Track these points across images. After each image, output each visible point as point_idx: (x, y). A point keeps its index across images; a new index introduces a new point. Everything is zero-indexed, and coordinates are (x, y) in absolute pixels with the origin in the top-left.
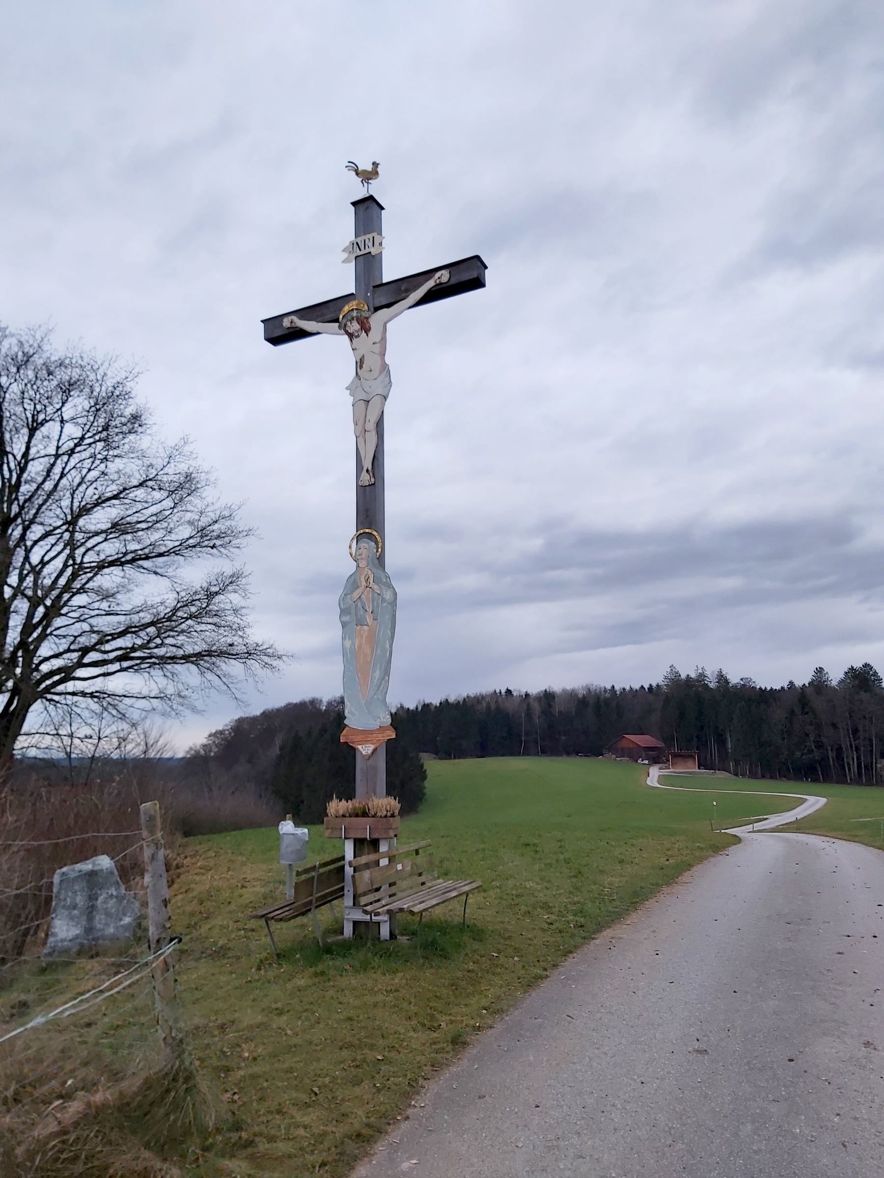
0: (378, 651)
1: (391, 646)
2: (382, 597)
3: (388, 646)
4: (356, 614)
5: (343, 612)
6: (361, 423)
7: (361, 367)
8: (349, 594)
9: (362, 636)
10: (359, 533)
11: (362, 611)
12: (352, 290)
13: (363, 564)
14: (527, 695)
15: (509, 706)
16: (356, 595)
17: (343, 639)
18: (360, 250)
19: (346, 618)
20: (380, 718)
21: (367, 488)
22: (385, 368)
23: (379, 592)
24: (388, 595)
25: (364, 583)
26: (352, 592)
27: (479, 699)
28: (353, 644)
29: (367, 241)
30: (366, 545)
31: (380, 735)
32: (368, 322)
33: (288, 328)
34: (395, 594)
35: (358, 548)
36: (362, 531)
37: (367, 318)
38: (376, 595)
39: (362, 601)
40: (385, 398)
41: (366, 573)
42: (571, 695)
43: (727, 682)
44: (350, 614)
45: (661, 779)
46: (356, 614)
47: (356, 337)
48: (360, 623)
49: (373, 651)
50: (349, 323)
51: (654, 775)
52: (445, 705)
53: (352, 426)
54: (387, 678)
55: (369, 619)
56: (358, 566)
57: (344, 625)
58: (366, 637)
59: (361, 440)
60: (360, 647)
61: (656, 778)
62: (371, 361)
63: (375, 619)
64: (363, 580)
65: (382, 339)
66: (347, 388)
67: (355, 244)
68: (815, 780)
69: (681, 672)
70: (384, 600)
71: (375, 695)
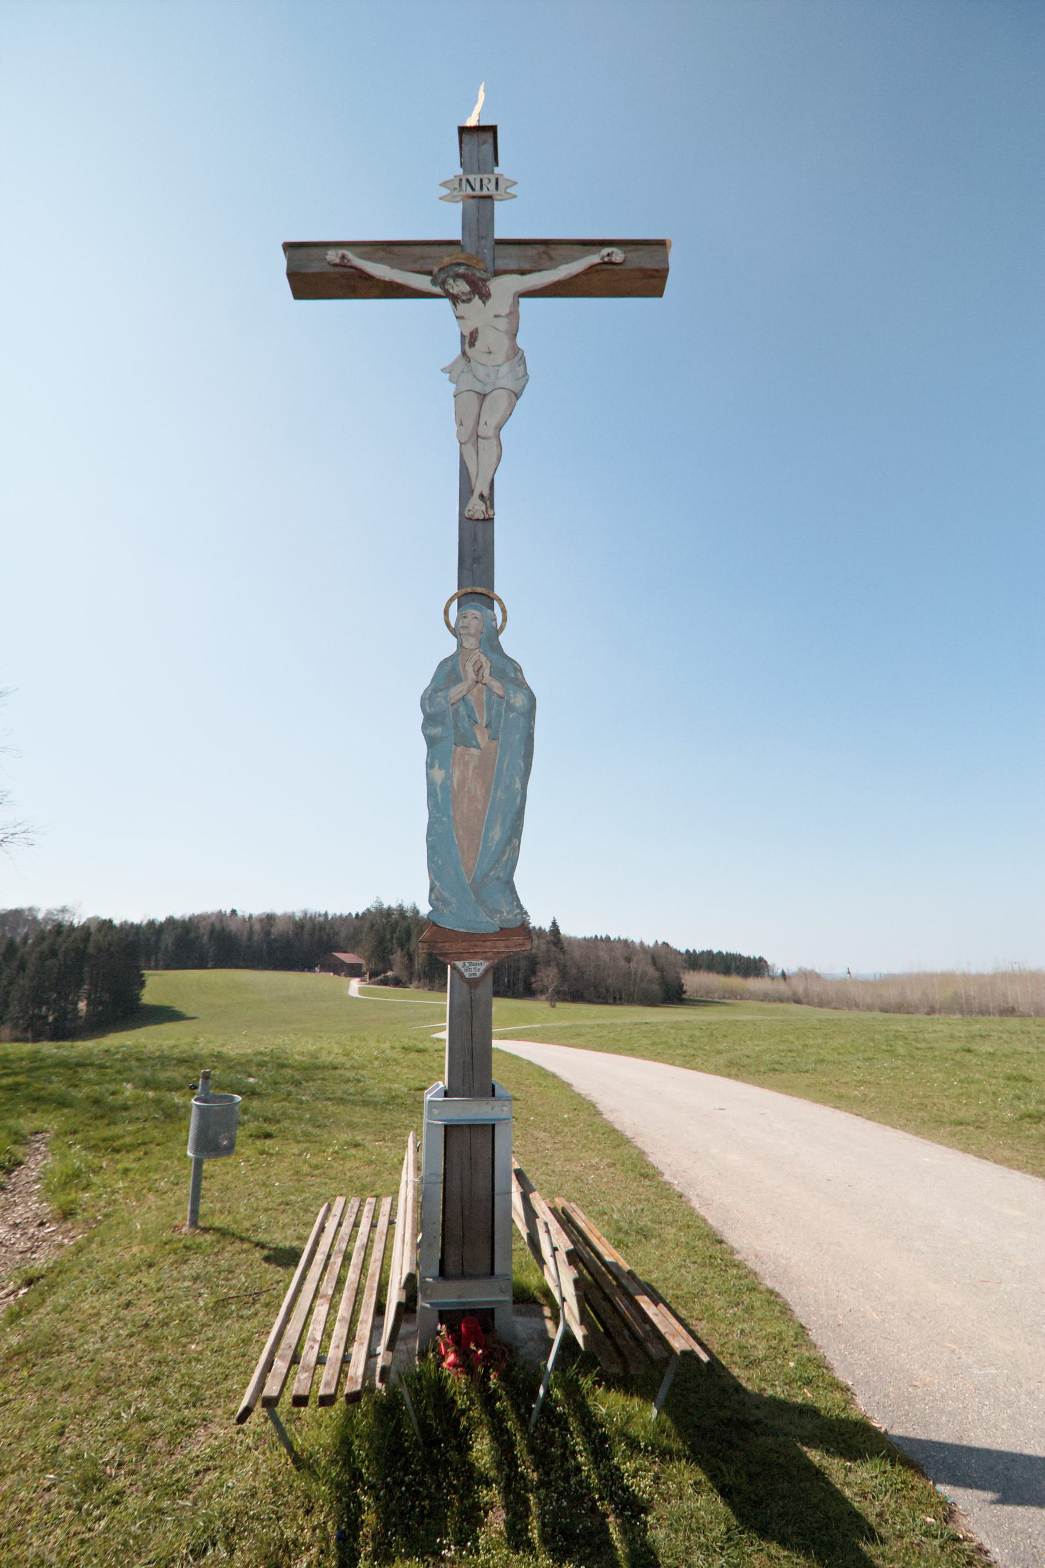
0: (499, 794)
1: (524, 788)
2: (508, 703)
3: (518, 786)
4: (456, 727)
5: (430, 720)
6: (470, 423)
7: (472, 344)
8: (441, 690)
9: (466, 765)
10: (463, 591)
11: (466, 724)
12: (456, 235)
13: (470, 643)
14: (250, 917)
15: (233, 927)
16: (456, 692)
17: (430, 766)
18: (481, 180)
19: (437, 731)
20: (502, 913)
21: (479, 523)
22: (516, 354)
23: (500, 693)
24: (519, 701)
25: (471, 675)
26: (447, 688)
27: (202, 918)
28: (449, 777)
29: (485, 182)
30: (478, 613)
31: (502, 944)
32: (486, 286)
33: (335, 265)
34: (532, 699)
35: (462, 616)
36: (469, 590)
37: (485, 280)
38: (494, 698)
39: (467, 705)
40: (517, 396)
41: (475, 657)
42: (290, 918)
43: (418, 912)
44: (443, 724)
45: (361, 991)
46: (456, 727)
47: (464, 301)
48: (465, 740)
49: (488, 791)
50: (451, 281)
51: (355, 986)
52: (170, 921)
53: (454, 428)
54: (515, 840)
55: (482, 737)
56: (460, 645)
57: (431, 742)
58: (475, 768)
59: (469, 449)
60: (463, 781)
61: (357, 991)
62: (492, 339)
63: (493, 738)
64: (470, 669)
65: (511, 313)
66: (443, 370)
67: (464, 182)
68: (673, 1003)
69: (384, 903)
70: (510, 707)
71: (491, 870)
